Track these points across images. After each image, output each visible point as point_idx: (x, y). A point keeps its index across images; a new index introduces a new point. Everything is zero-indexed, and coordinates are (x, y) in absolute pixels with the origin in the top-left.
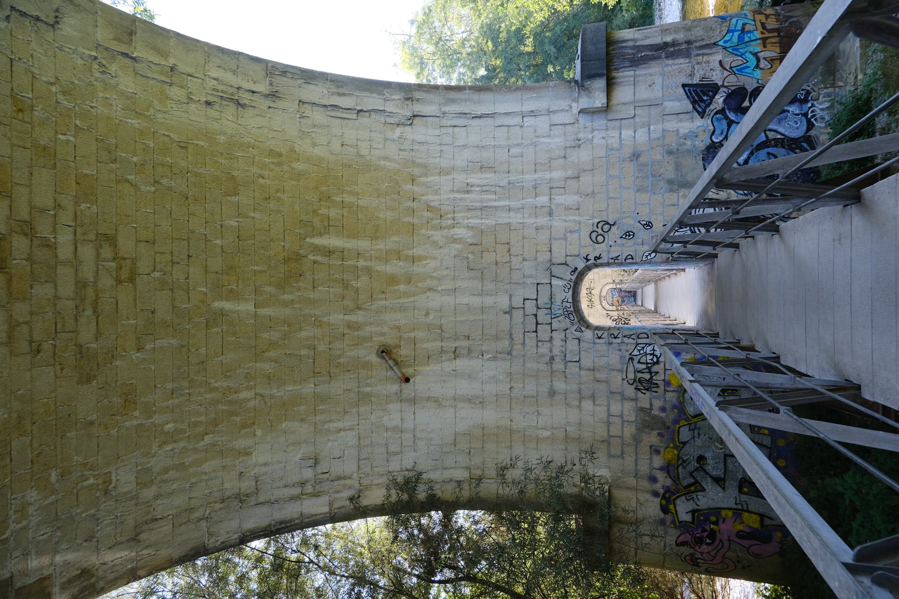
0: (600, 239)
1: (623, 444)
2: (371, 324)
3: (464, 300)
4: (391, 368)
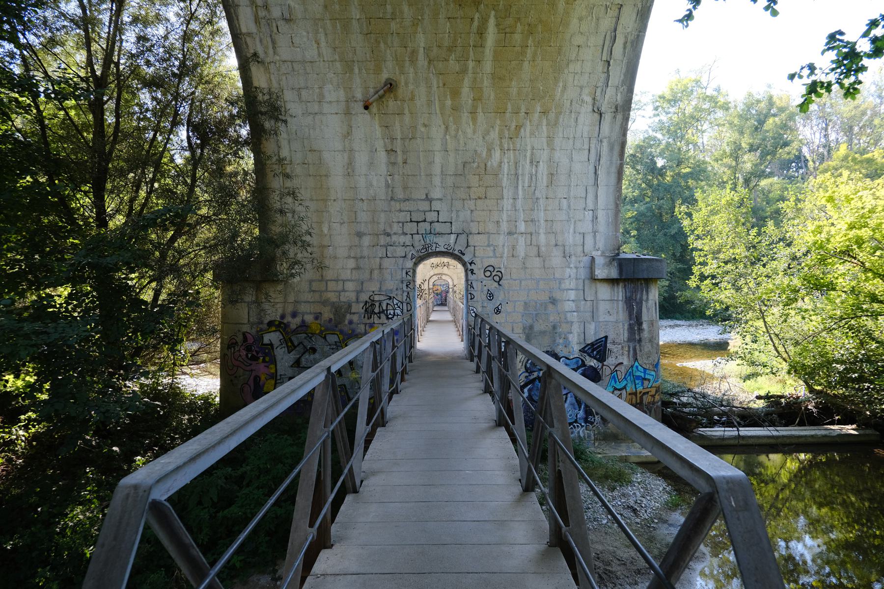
0: (488, 274)
1: (321, 292)
2: (416, 73)
3: (438, 159)
4: (377, 92)
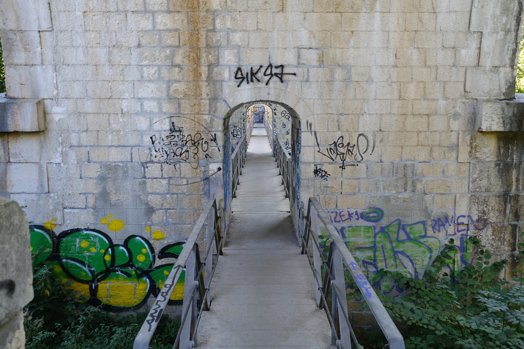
0: (283, 115)
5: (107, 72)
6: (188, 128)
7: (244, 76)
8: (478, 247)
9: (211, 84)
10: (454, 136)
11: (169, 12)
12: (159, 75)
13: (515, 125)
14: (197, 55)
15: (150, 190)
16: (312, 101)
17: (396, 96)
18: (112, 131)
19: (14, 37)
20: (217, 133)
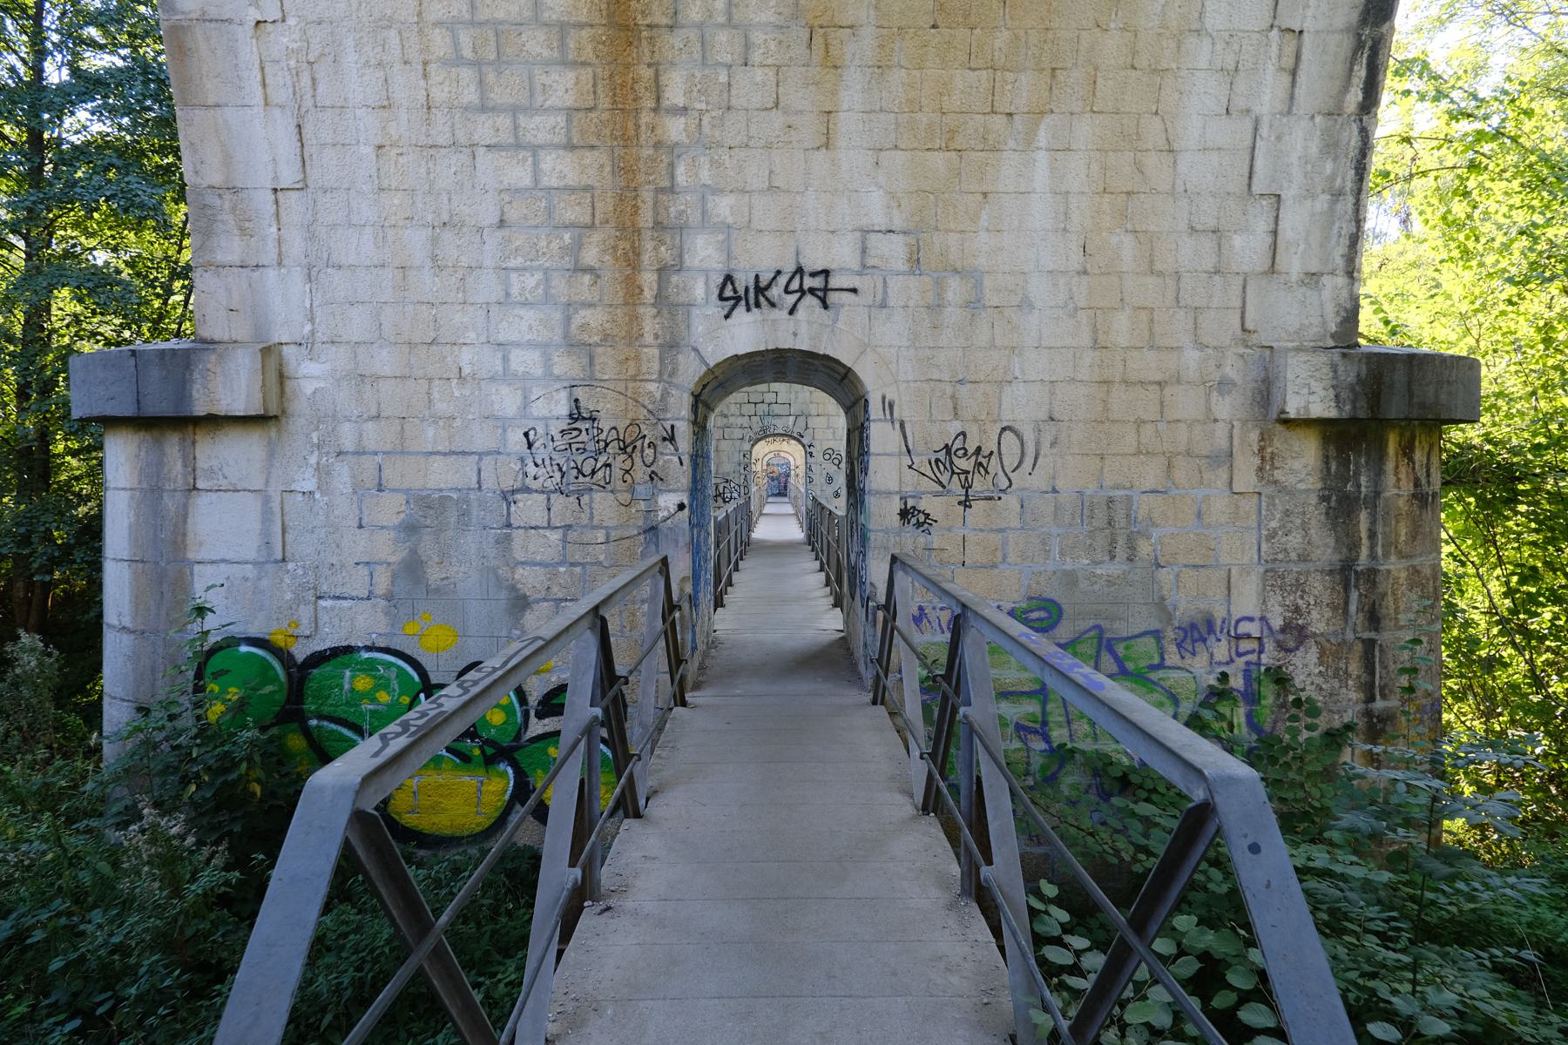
5: (427, 283)
6: (610, 413)
7: (742, 295)
8: (1287, 692)
9: (665, 312)
10: (1221, 431)
11: (570, 147)
12: (546, 293)
13: (1362, 403)
14: (633, 247)
15: (519, 555)
16: (893, 351)
17: (1086, 339)
18: (436, 419)
19: (219, 202)
20: (678, 424)
